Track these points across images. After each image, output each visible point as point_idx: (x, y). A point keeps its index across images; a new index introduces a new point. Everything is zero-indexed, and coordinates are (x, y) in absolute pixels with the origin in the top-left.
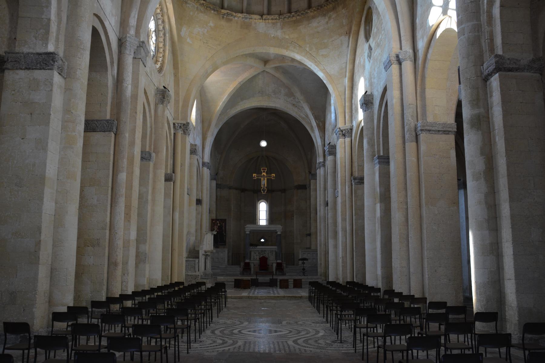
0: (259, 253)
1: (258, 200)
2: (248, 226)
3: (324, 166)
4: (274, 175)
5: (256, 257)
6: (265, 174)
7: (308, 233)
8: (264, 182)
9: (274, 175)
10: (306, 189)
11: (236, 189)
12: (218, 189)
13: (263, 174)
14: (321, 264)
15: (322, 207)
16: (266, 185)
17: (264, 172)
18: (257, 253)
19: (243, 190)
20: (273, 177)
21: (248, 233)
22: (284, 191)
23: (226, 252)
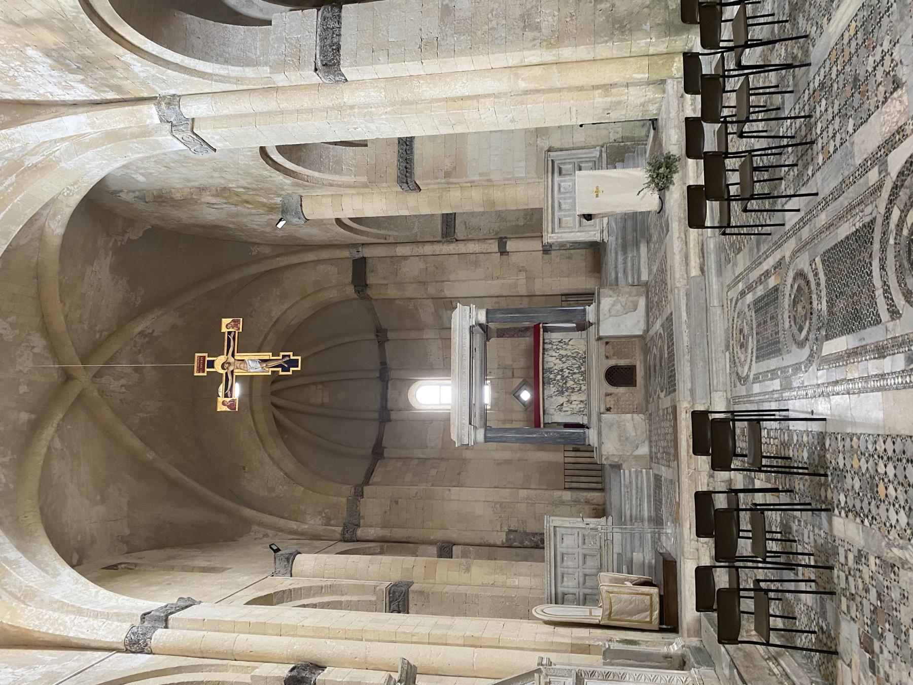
0: (561, 393)
1: (409, 407)
2: (454, 437)
3: (173, 100)
4: (225, 321)
5: (576, 406)
6: (219, 360)
7: (494, 247)
8: (253, 364)
9: (225, 321)
10: (364, 259)
11: (370, 472)
12: (360, 533)
13: (218, 368)
14: (607, 88)
15: (348, 96)
16: (267, 355)
17: (211, 364)
18: (561, 400)
19: (378, 452)
20: (236, 322)
21: (480, 435)
22: (381, 335)
23: (556, 521)
